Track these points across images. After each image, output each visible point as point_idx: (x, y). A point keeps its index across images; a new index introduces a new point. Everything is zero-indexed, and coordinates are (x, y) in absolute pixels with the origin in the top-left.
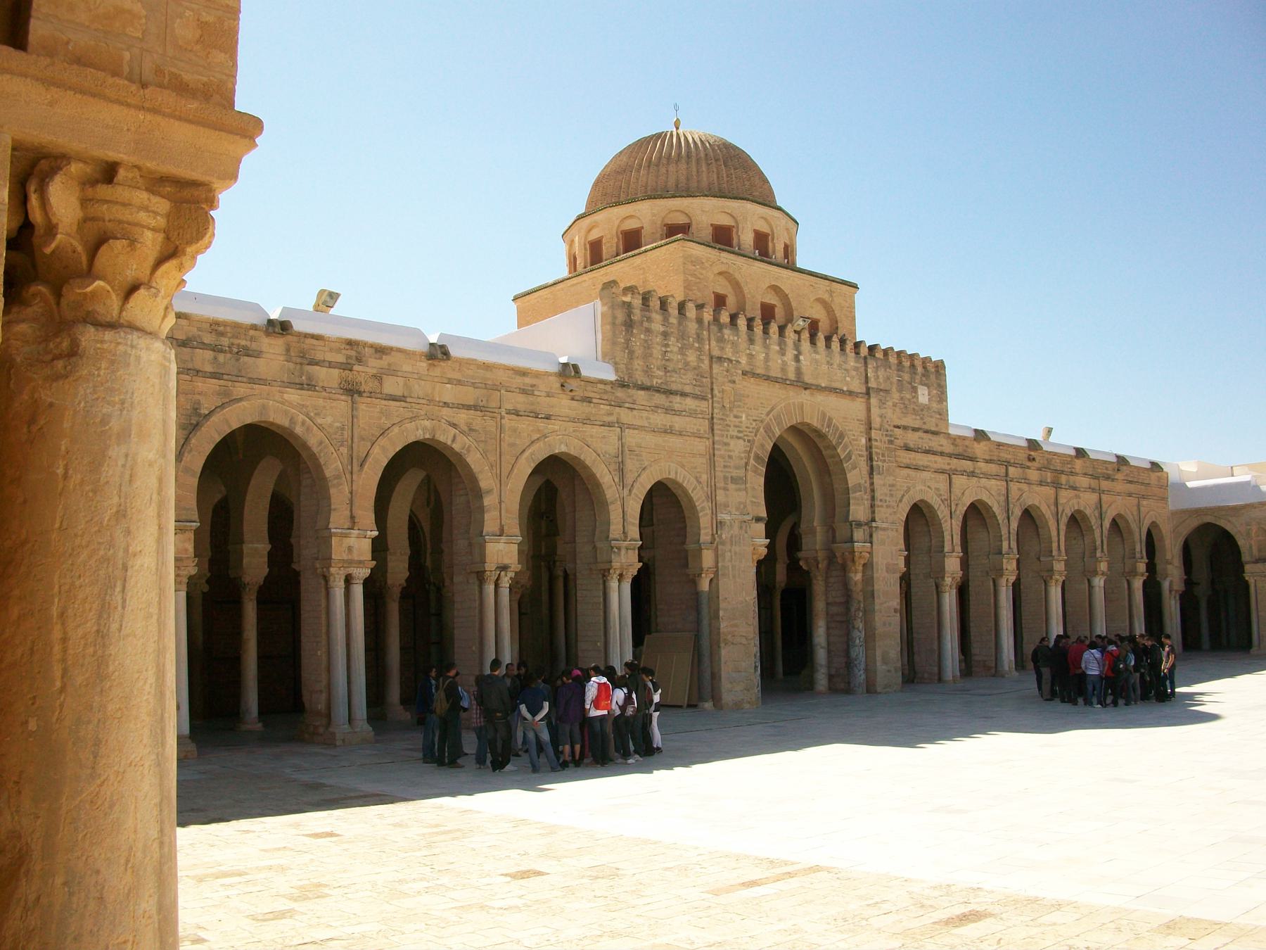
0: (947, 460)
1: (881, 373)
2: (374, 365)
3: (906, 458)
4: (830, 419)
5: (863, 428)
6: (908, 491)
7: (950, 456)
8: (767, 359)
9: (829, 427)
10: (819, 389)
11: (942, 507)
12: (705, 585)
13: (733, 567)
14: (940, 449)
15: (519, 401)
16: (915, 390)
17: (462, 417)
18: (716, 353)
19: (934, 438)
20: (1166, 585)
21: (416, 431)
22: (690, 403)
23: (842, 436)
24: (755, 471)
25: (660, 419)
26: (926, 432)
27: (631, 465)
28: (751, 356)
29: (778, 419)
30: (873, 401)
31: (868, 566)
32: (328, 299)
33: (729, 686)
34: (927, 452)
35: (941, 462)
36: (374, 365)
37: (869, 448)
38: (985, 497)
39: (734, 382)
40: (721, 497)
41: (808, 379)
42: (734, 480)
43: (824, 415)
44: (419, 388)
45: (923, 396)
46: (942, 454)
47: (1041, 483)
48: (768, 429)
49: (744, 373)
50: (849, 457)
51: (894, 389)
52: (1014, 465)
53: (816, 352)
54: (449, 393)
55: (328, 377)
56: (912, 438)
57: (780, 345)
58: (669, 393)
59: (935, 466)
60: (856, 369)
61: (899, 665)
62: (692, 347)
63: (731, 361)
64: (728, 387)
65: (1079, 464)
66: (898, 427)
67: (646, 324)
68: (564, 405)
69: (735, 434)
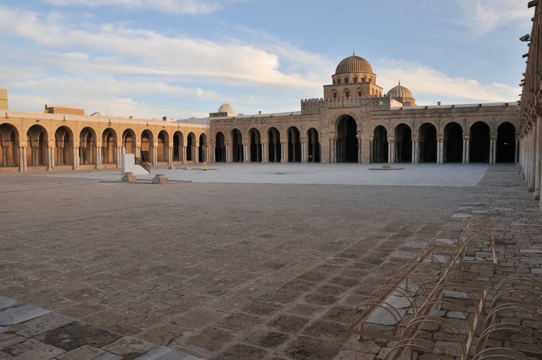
2: (265, 119)
3: (374, 117)
15: (285, 120)
17: (276, 124)
20: (516, 142)
21: (271, 126)
25: (309, 119)
27: (304, 126)
30: (363, 107)
32: (260, 112)
35: (387, 117)
36: (265, 119)
38: (404, 123)
40: (322, 130)
41: (345, 106)
44: (271, 121)
45: (381, 103)
47: (430, 117)
48: (335, 117)
49: (328, 108)
52: (418, 114)
54: (275, 121)
55: (259, 122)
65: (453, 110)
68: (292, 120)
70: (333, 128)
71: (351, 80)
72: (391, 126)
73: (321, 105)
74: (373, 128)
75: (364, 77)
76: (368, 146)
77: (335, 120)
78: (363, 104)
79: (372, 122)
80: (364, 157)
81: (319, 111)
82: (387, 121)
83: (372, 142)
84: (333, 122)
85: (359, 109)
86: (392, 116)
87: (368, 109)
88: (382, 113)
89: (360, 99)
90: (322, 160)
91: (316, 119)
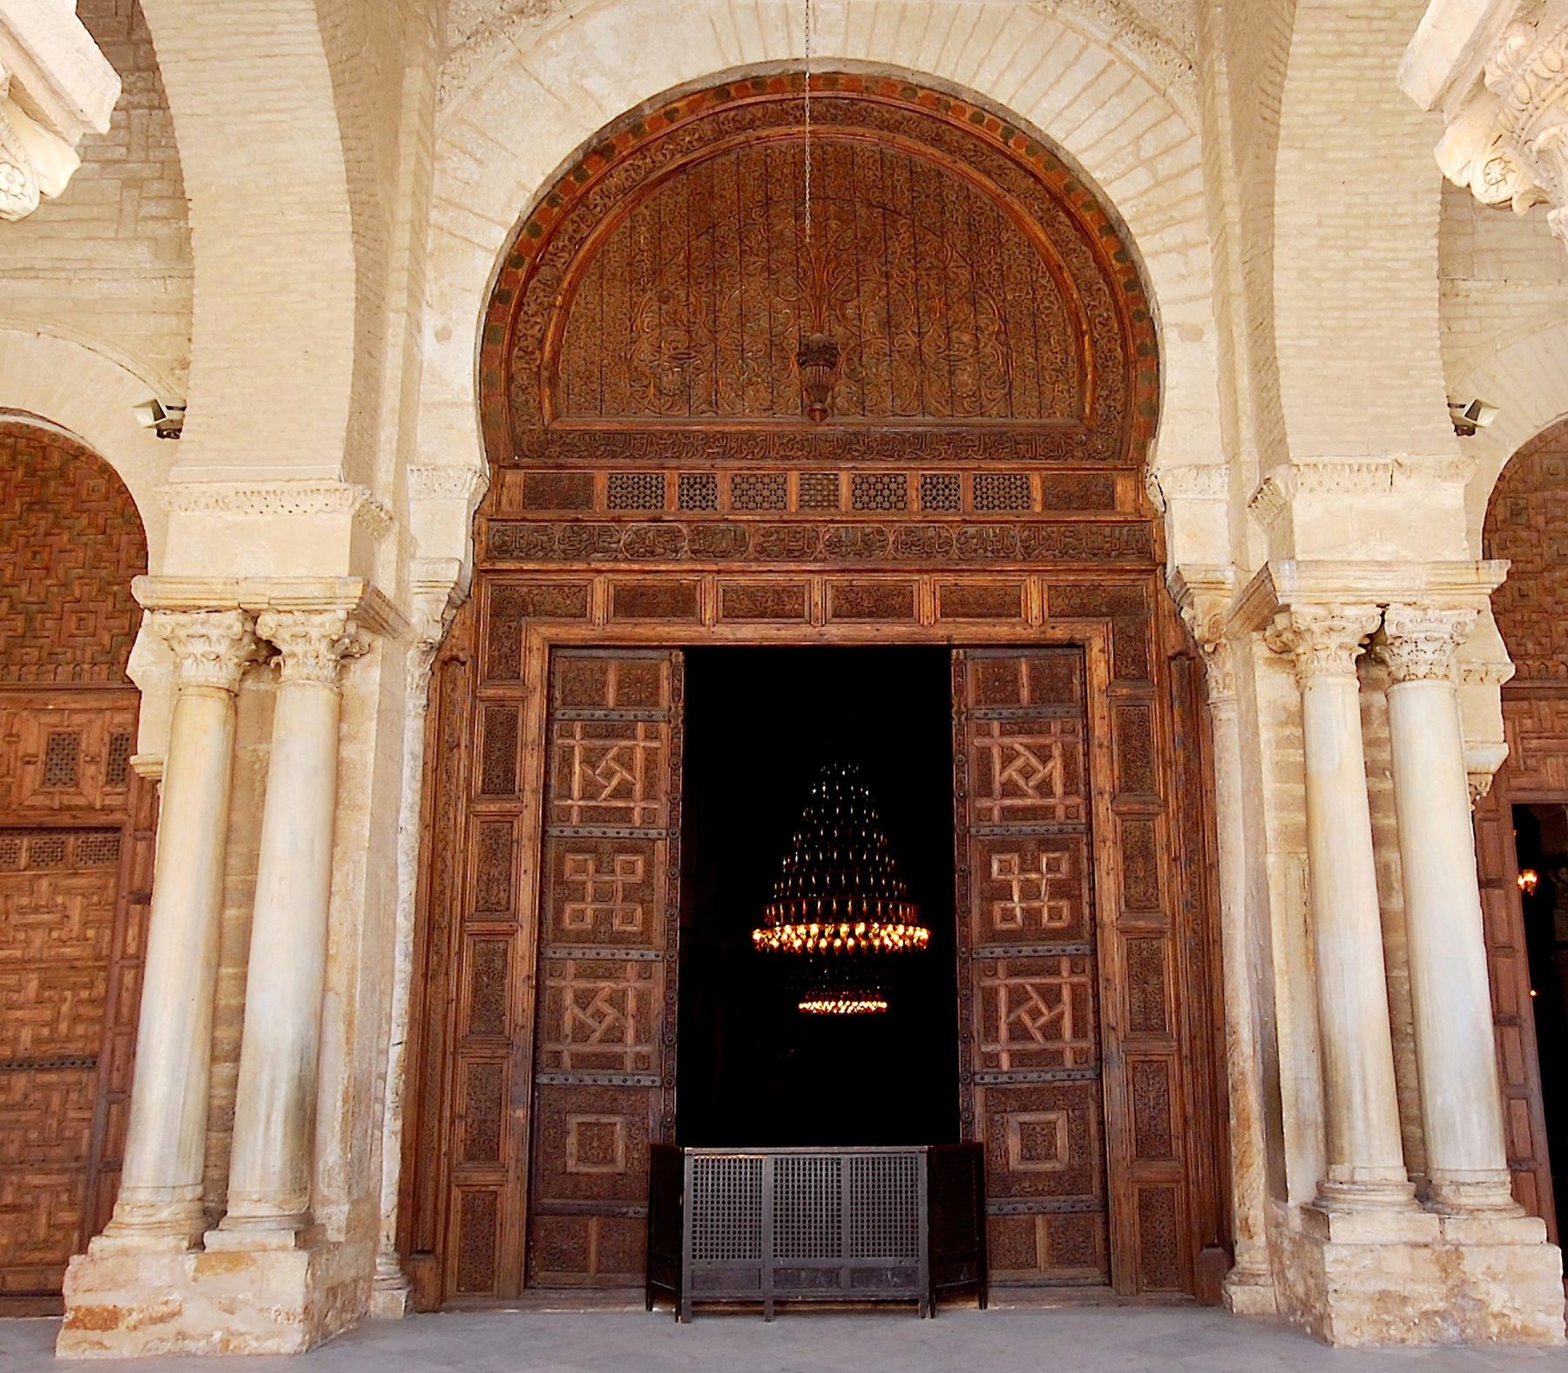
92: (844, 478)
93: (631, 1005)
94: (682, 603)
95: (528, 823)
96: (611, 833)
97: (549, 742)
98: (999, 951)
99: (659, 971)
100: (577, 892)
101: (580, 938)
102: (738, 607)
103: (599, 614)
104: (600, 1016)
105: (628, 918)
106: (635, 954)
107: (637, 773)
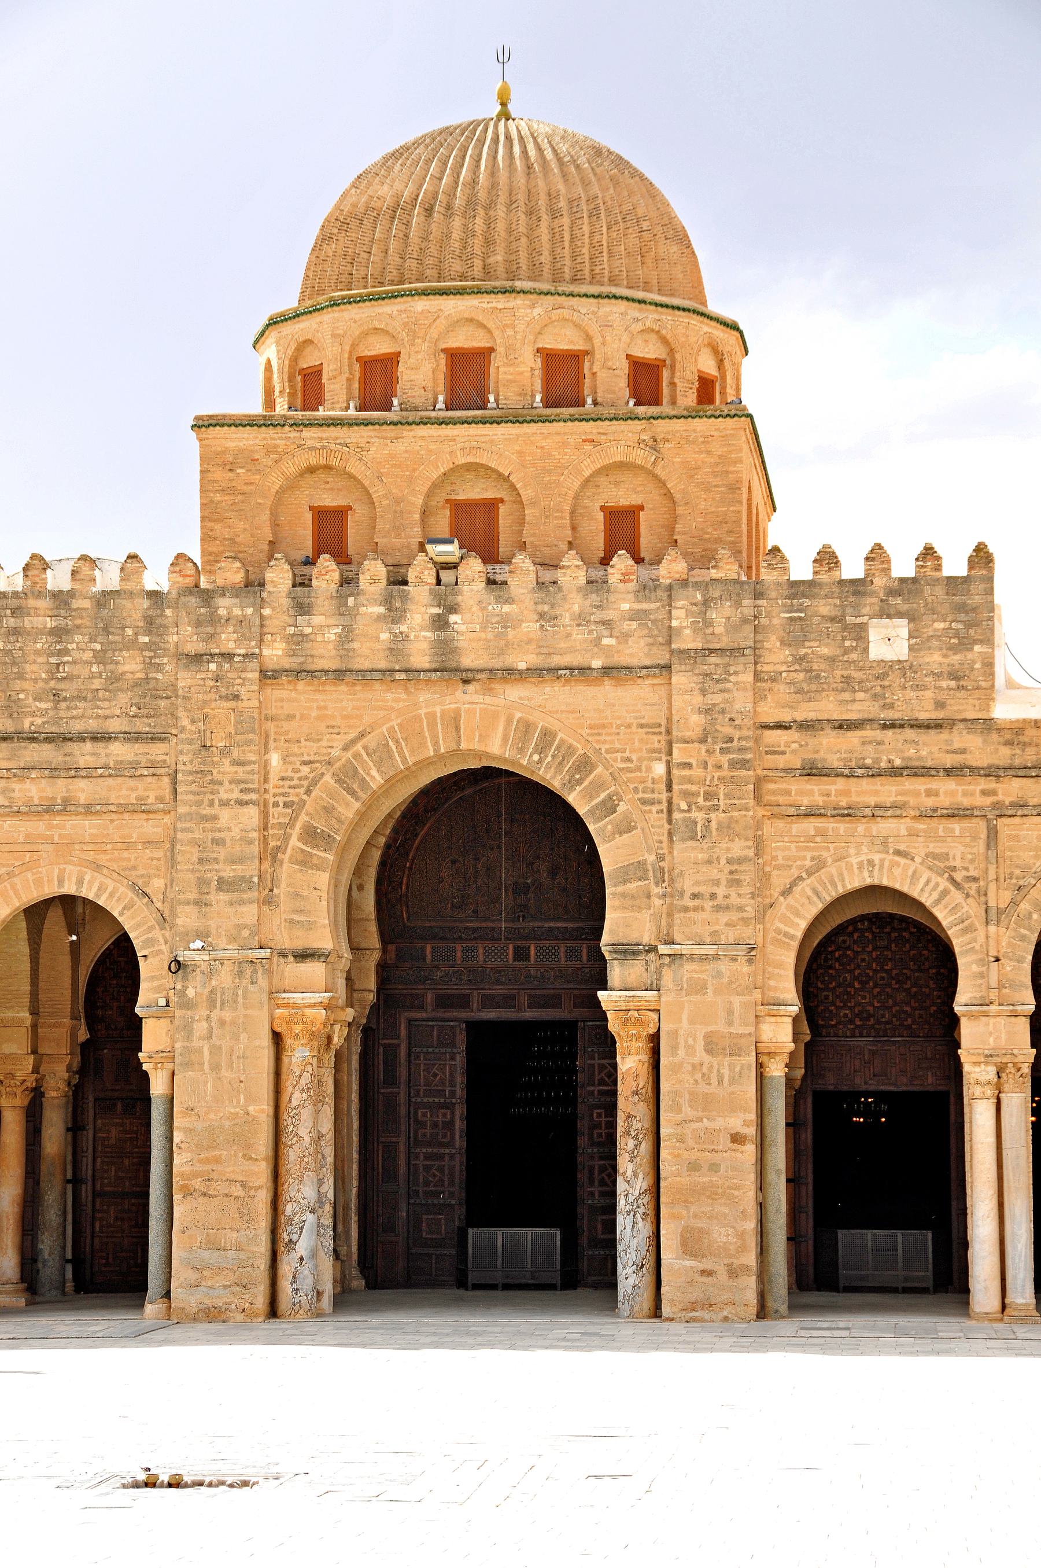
0: (984, 784)
1: (720, 616)
4: (547, 735)
5: (657, 741)
6: (820, 865)
7: (992, 772)
8: (347, 635)
9: (541, 750)
10: (509, 671)
11: (957, 896)
12: (158, 1087)
13: (215, 1050)
14: (949, 761)
16: (860, 633)
18: (194, 646)
19: (932, 736)
22: (119, 751)
23: (585, 765)
24: (304, 861)
25: (34, 790)
26: (893, 726)
28: (298, 640)
29: (382, 754)
30: (679, 679)
31: (655, 1039)
33: (193, 1276)
34: (895, 772)
35: (950, 792)
37: (669, 788)
39: (236, 697)
40: (186, 918)
42: (223, 885)
43: (527, 727)
45: (888, 641)
46: (949, 772)
48: (348, 778)
49: (268, 675)
50: (609, 807)
51: (772, 642)
53: (509, 601)
56: (831, 748)
57: (387, 601)
58: (67, 738)
59: (930, 802)
60: (635, 616)
61: (751, 1259)
62: (132, 644)
63: (228, 656)
64: (220, 709)
66: (780, 726)
67: (12, 622)
69: (236, 795)
70: (315, 906)
71: (516, 375)
72: (1000, 897)
73: (185, 636)
74: (796, 918)
75: (649, 351)
76: (744, 1121)
77: (349, 809)
78: (688, 640)
79: (788, 844)
80: (690, 1247)
81: (148, 691)
82: (961, 844)
83: (777, 1070)
84: (311, 835)
85: (637, 700)
86: (1011, 789)
87: (742, 702)
88: (896, 747)
89: (647, 589)
90: (180, 1274)
91: (122, 790)
92: (532, 948)
93: (447, 1172)
94: (464, 1002)
95: (402, 1098)
96: (436, 1100)
97: (410, 1062)
98: (595, 1150)
99: (458, 1157)
100: (423, 1124)
101: (429, 1144)
102: (489, 1002)
103: (429, 1008)
104: (435, 1176)
105: (445, 1136)
106: (447, 1151)
107: (446, 1073)
